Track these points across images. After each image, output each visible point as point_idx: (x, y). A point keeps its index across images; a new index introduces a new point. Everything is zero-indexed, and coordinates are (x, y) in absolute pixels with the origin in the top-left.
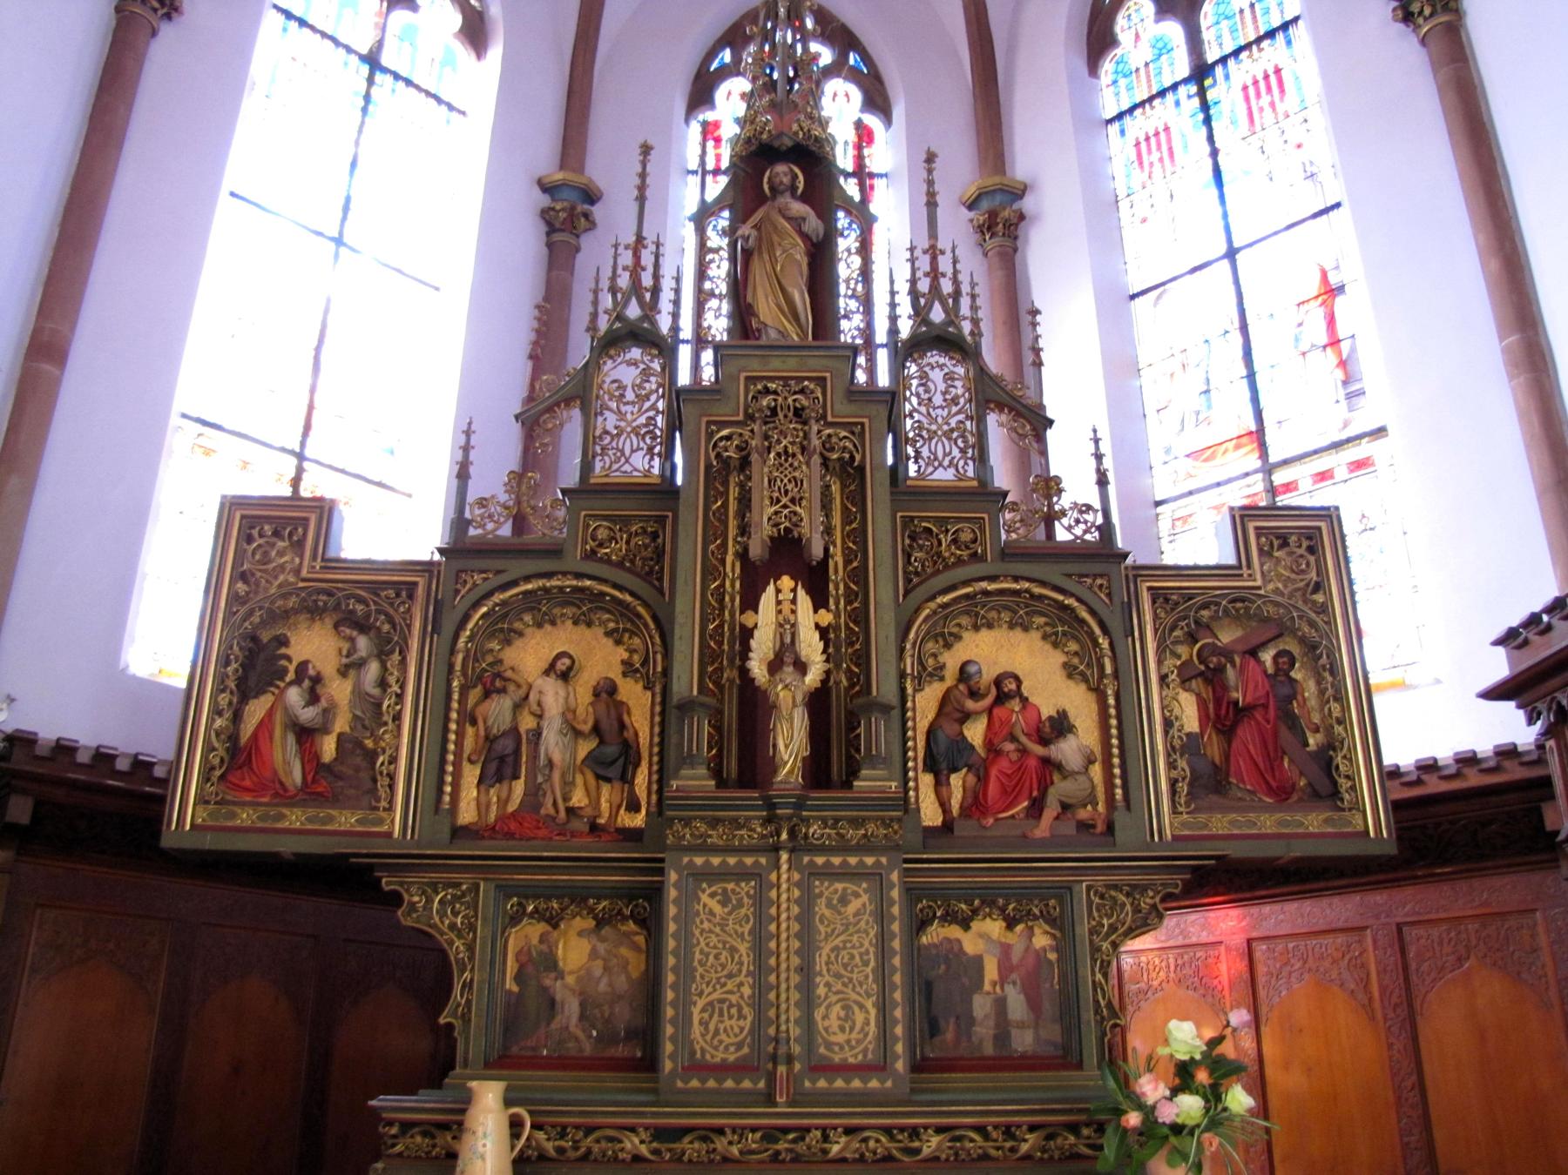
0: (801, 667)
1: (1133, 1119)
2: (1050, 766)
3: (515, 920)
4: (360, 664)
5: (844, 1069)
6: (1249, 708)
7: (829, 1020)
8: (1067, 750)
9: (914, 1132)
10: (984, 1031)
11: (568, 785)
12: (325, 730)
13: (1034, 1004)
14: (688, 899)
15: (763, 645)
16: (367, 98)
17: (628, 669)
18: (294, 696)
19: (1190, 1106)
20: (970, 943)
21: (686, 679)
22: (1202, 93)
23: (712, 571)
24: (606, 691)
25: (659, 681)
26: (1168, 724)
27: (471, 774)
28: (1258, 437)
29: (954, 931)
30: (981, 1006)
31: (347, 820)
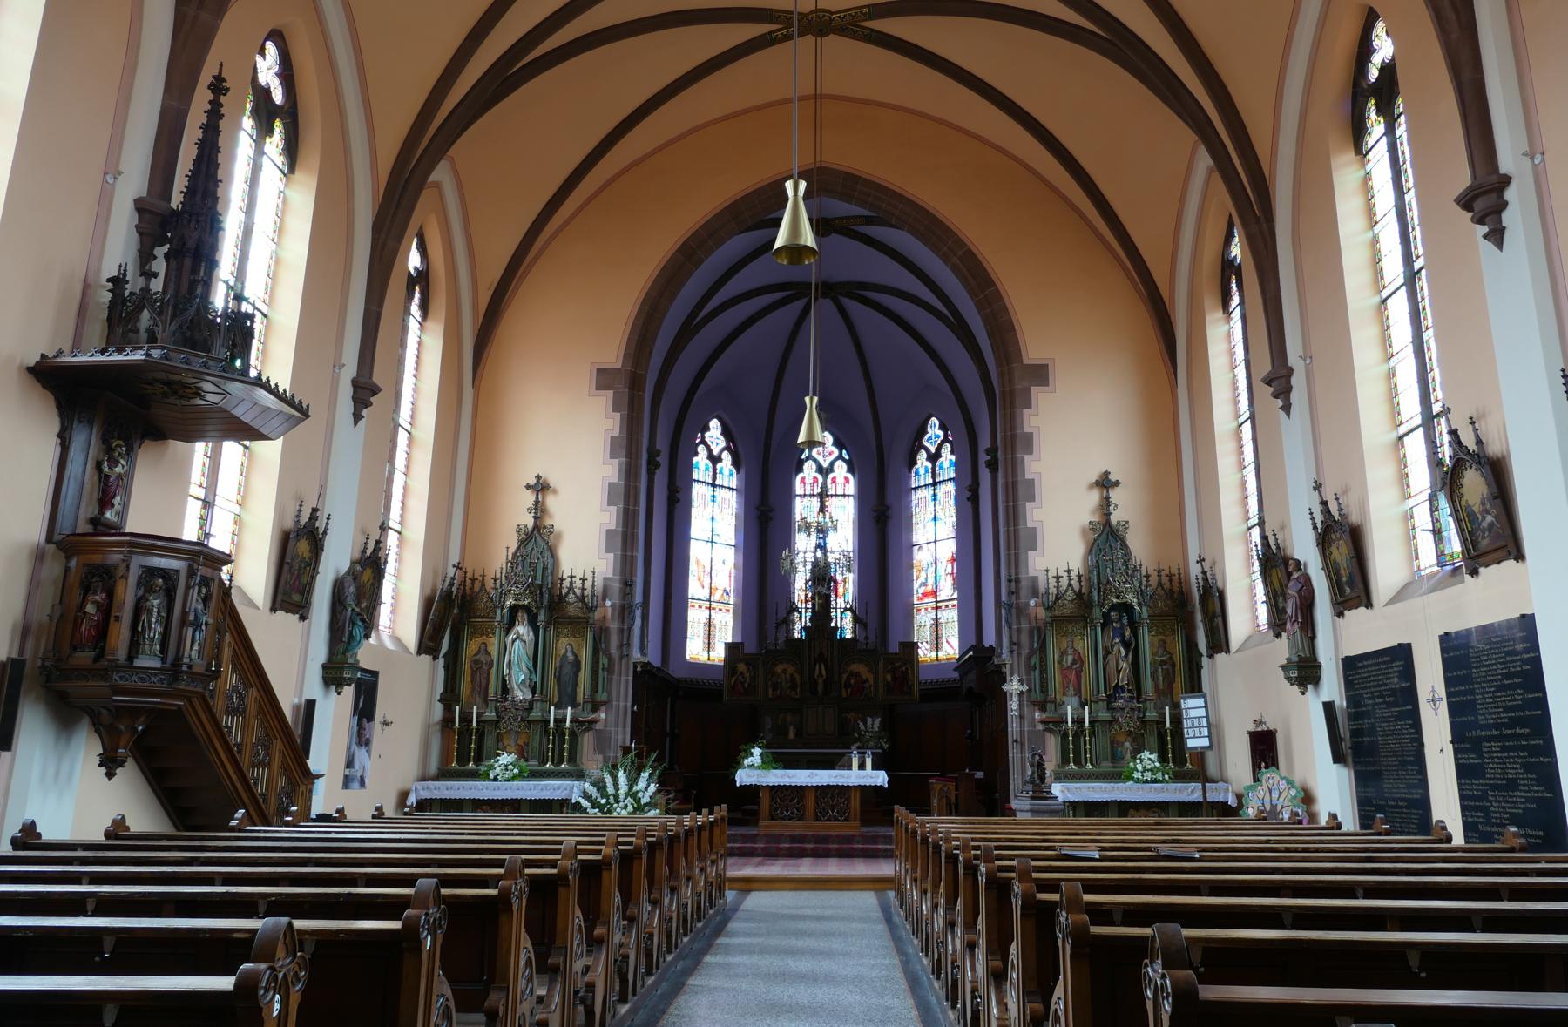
0: (822, 676)
8: (867, 685)
12: (745, 682)
15: (817, 672)
18: (740, 677)
22: (934, 490)
23: (810, 657)
24: (792, 675)
26: (884, 681)
28: (935, 593)
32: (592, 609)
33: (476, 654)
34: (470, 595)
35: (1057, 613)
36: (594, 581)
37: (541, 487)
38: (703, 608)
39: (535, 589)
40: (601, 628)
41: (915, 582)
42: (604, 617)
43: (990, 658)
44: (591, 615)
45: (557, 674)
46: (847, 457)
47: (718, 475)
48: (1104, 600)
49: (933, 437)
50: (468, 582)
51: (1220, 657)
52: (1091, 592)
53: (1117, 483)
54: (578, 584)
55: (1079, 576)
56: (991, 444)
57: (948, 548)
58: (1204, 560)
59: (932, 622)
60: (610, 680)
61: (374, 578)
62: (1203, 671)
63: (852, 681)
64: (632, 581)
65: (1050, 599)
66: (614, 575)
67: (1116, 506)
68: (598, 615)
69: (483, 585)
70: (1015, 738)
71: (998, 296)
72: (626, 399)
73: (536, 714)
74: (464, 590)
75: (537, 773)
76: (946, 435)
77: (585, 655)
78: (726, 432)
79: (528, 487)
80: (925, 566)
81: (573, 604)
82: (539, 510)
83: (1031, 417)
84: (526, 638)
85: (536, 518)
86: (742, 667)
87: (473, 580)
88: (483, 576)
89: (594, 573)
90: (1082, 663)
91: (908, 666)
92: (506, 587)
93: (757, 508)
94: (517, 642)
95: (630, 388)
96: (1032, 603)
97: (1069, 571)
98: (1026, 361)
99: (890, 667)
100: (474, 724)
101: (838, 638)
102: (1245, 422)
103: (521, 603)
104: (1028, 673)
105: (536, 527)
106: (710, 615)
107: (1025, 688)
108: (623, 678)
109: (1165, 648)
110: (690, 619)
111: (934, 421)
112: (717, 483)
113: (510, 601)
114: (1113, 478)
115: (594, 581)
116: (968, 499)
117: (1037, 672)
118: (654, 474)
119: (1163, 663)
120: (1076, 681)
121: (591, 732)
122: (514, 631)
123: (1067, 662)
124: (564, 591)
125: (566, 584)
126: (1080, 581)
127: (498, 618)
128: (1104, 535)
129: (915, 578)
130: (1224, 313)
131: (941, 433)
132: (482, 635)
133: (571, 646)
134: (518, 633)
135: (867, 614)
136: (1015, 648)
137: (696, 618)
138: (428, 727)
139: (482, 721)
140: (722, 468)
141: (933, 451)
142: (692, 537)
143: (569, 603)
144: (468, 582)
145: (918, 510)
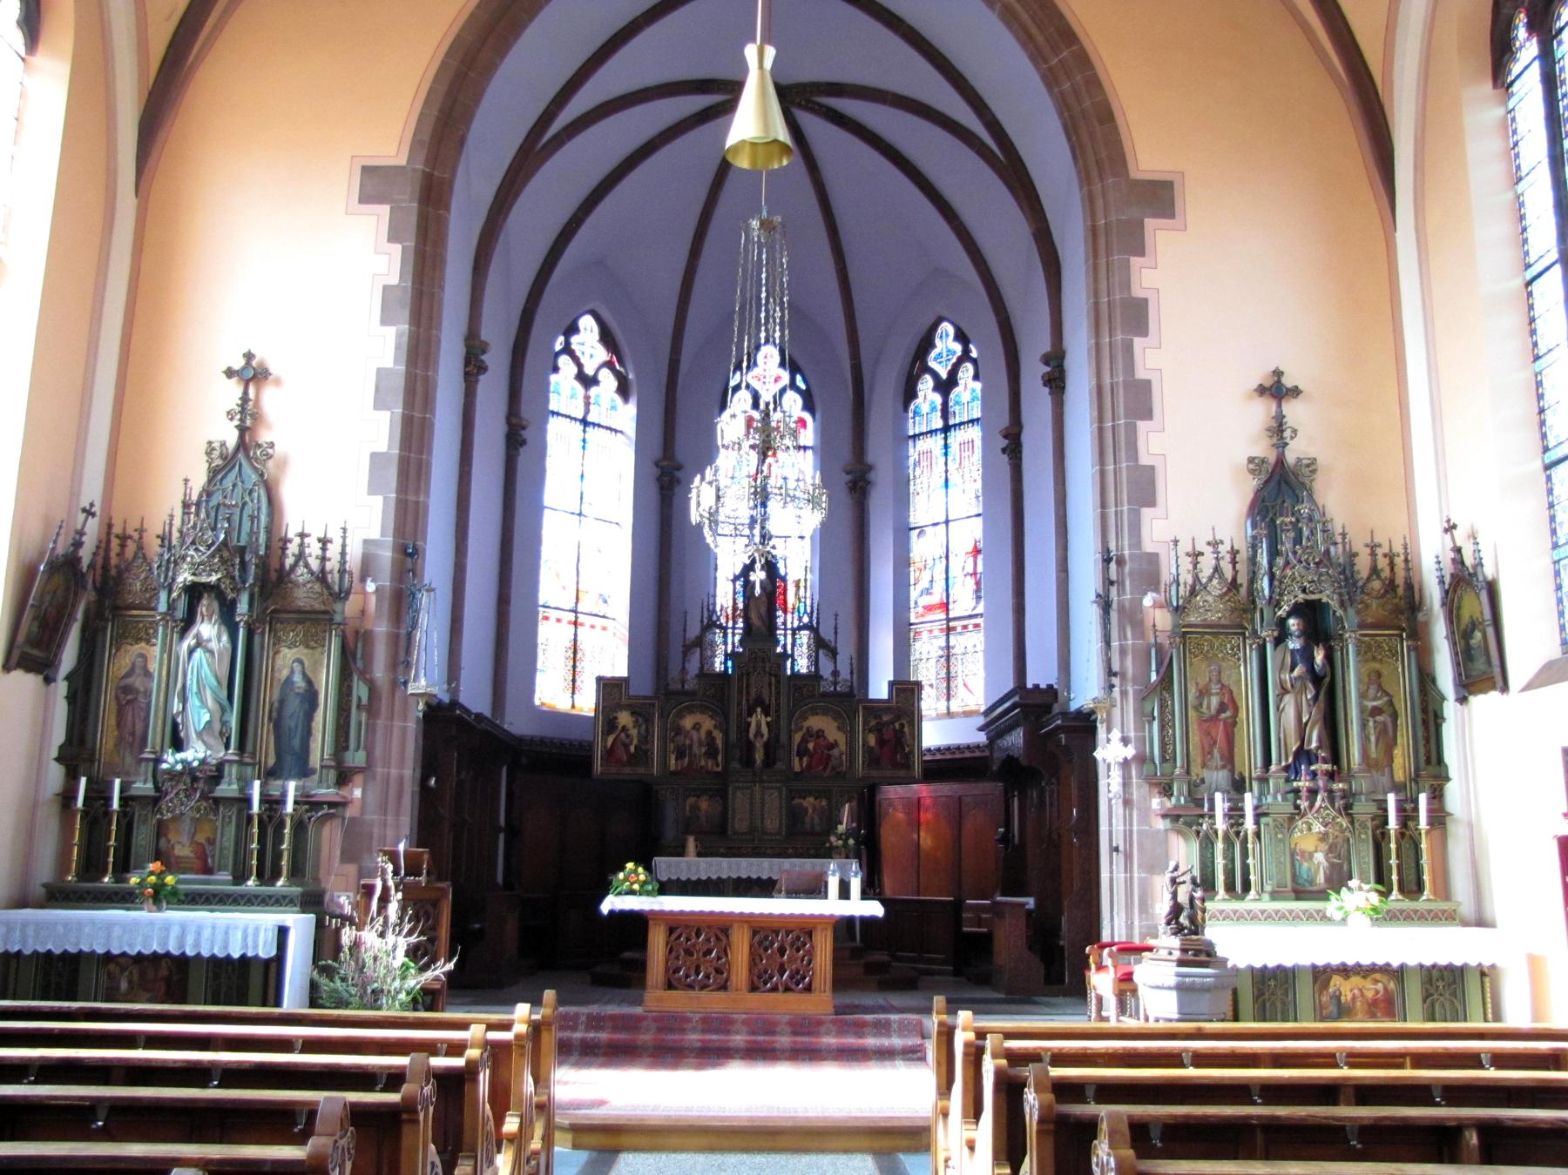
0: (762, 736)
1: (828, 845)
2: (829, 756)
3: (688, 797)
4: (640, 726)
5: (771, 834)
6: (888, 741)
7: (768, 823)
8: (835, 752)
9: (787, 848)
10: (808, 826)
11: (700, 760)
13: (820, 819)
14: (734, 793)
16: (584, 441)
17: (715, 727)
18: (623, 735)
19: (840, 842)
20: (805, 803)
21: (733, 736)
22: (946, 438)
23: (740, 704)
24: (709, 733)
25: (726, 733)
26: (864, 745)
27: (673, 757)
28: (945, 606)
29: (802, 801)
30: (807, 820)
31: (641, 770)
32: (342, 595)
33: (128, 675)
34: (116, 566)
35: (1193, 619)
36: (344, 546)
37: (253, 374)
38: (565, 622)
39: (231, 553)
40: (357, 632)
41: (912, 588)
42: (363, 612)
43: (1047, 708)
44: (338, 607)
45: (274, 714)
46: (803, 386)
47: (592, 407)
48: (1281, 595)
49: (944, 355)
50: (115, 543)
51: (1484, 703)
52: (1253, 579)
53: (1295, 392)
54: (314, 549)
55: (1234, 553)
56: (1053, 345)
57: (970, 532)
58: (1454, 527)
59: (941, 653)
60: (371, 729)
61: (67, 589)
62: (1445, 727)
63: (811, 746)
64: (415, 547)
65: (1181, 592)
66: (383, 534)
67: (1295, 431)
68: (351, 607)
69: (140, 547)
70: (1114, 845)
71: (1083, 60)
72: (413, 219)
73: (228, 788)
74: (107, 558)
75: (215, 896)
76: (966, 351)
77: (326, 681)
78: (607, 338)
79: (230, 373)
80: (930, 562)
81: (304, 585)
82: (248, 418)
83: (1143, 270)
84: (214, 645)
85: (243, 430)
86: (624, 718)
87: (124, 539)
88: (141, 531)
89: (344, 530)
90: (1236, 710)
91: (904, 722)
92: (178, 552)
93: (657, 464)
94: (198, 653)
95: (420, 202)
96: (1148, 601)
97: (1215, 544)
98: (1135, 174)
99: (873, 723)
100: (116, 805)
101: (789, 672)
102: (1547, 269)
103: (204, 579)
104: (1139, 727)
105: (242, 445)
106: (576, 635)
107: (1130, 752)
108: (397, 723)
109: (1380, 687)
110: (541, 639)
111: (947, 328)
112: (590, 418)
113: (184, 577)
114: (1288, 382)
115: (344, 546)
116: (1004, 451)
117: (1156, 724)
118: (477, 382)
119: (1376, 711)
120: (1224, 745)
121: (337, 823)
122: (194, 631)
123: (1209, 707)
124: (289, 561)
125: (293, 548)
126: (1234, 562)
127: (163, 607)
128: (1273, 483)
129: (912, 582)
130: (1495, 85)
131: (958, 348)
132: (138, 640)
133: (301, 662)
134: (198, 636)
135: (836, 633)
136: (1116, 681)
137: (552, 638)
138: (31, 808)
139: (133, 798)
140: (597, 396)
141: (944, 375)
142: (546, 503)
143: (296, 584)
144: (115, 543)
145: (918, 470)
